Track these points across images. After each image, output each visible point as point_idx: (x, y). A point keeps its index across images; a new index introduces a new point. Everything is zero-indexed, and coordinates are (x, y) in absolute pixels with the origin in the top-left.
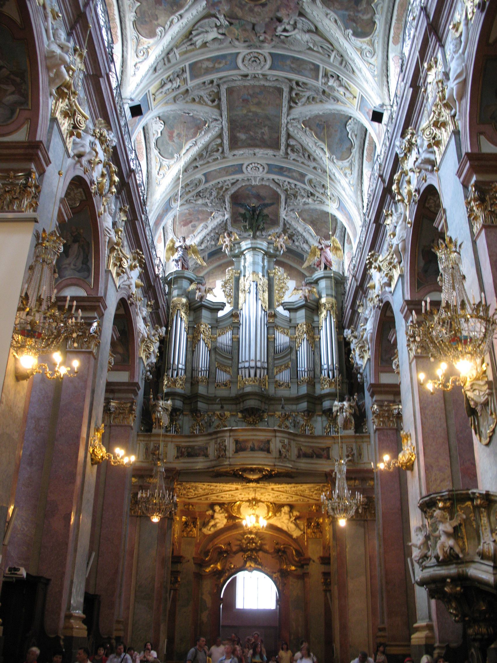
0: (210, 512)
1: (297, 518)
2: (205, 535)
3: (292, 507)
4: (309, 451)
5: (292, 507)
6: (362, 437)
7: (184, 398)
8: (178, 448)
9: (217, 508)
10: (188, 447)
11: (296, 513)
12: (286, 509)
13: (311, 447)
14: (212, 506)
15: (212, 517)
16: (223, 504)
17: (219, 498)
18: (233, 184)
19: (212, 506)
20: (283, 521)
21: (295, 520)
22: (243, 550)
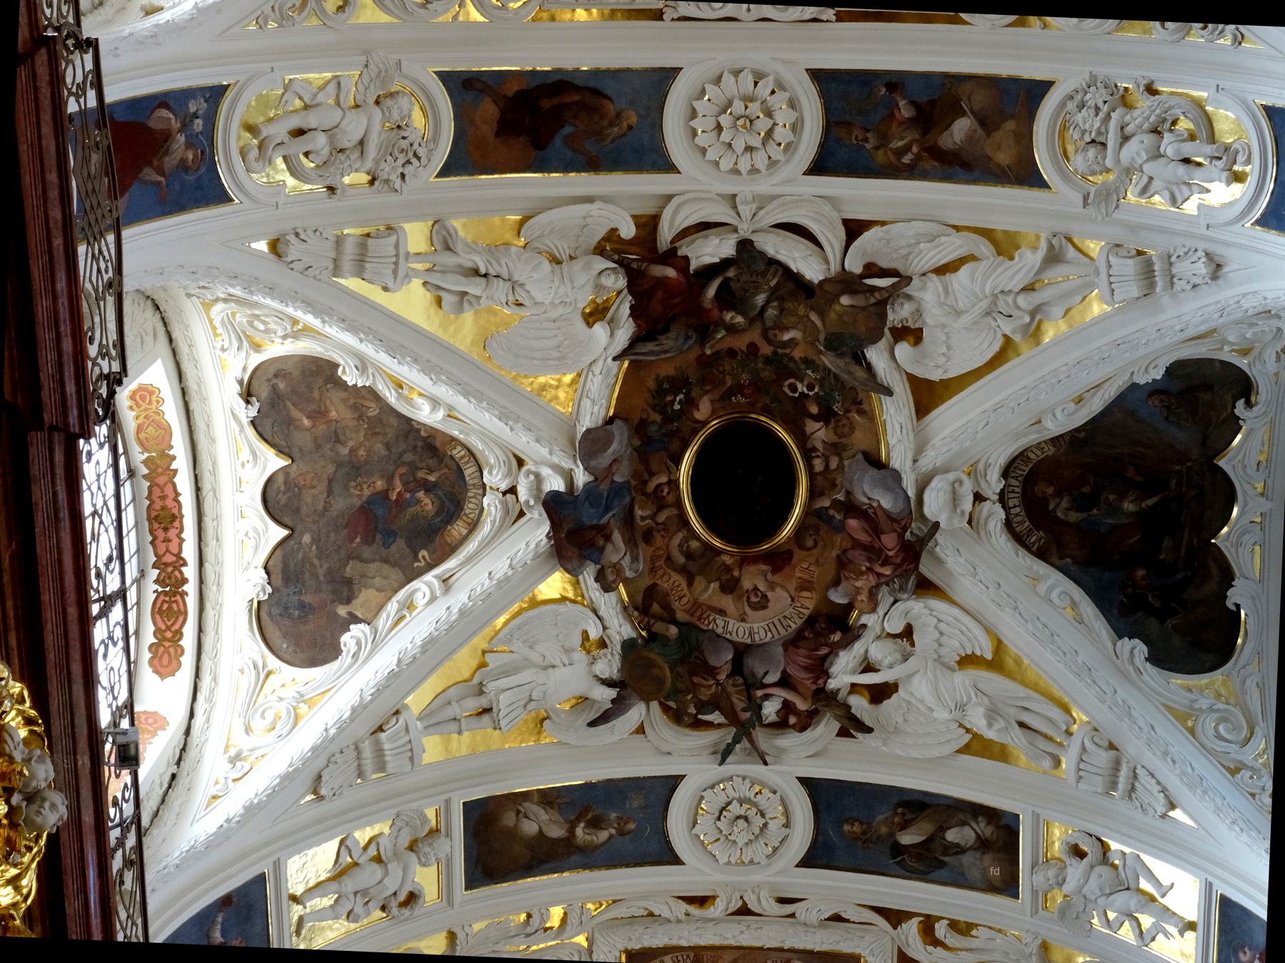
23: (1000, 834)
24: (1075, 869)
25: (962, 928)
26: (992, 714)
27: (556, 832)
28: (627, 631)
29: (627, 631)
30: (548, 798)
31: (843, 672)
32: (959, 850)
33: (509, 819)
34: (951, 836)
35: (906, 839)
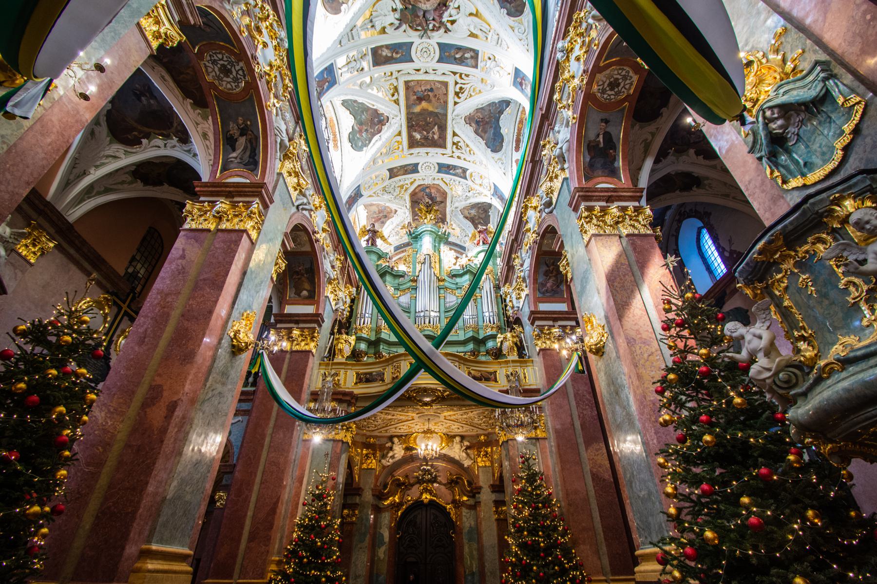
0: (389, 444)
1: (468, 448)
2: (384, 467)
3: (463, 438)
4: (478, 375)
5: (463, 438)
6: (526, 362)
7: (370, 343)
8: (357, 374)
9: (396, 440)
10: (366, 374)
11: (466, 443)
12: (458, 439)
13: (479, 371)
14: (391, 438)
15: (391, 449)
16: (402, 436)
17: (398, 430)
18: (412, 183)
19: (391, 438)
20: (456, 451)
21: (466, 449)
22: (420, 482)
23: (476, 53)
24: (489, 62)
25: (467, 76)
26: (475, 27)
27: (389, 55)
28: (401, 7)
29: (401, 7)
30: (387, 47)
31: (445, 18)
32: (467, 59)
33: (380, 52)
34: (466, 55)
35: (457, 56)
